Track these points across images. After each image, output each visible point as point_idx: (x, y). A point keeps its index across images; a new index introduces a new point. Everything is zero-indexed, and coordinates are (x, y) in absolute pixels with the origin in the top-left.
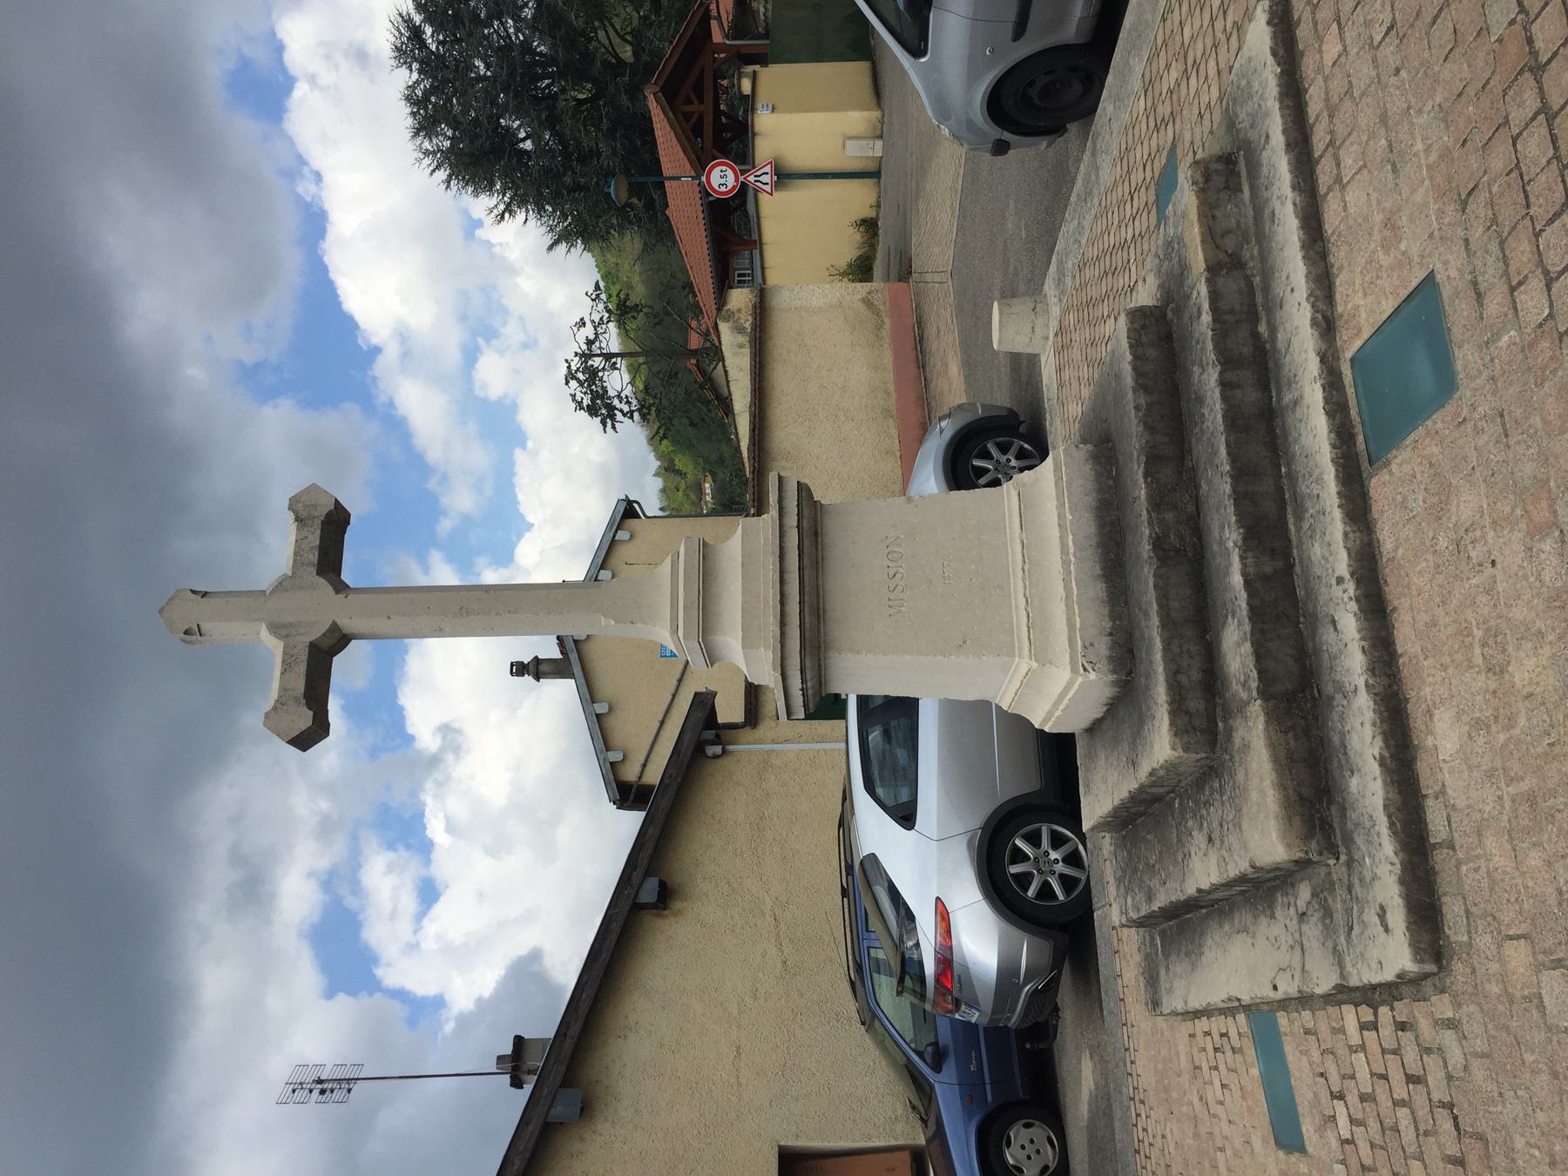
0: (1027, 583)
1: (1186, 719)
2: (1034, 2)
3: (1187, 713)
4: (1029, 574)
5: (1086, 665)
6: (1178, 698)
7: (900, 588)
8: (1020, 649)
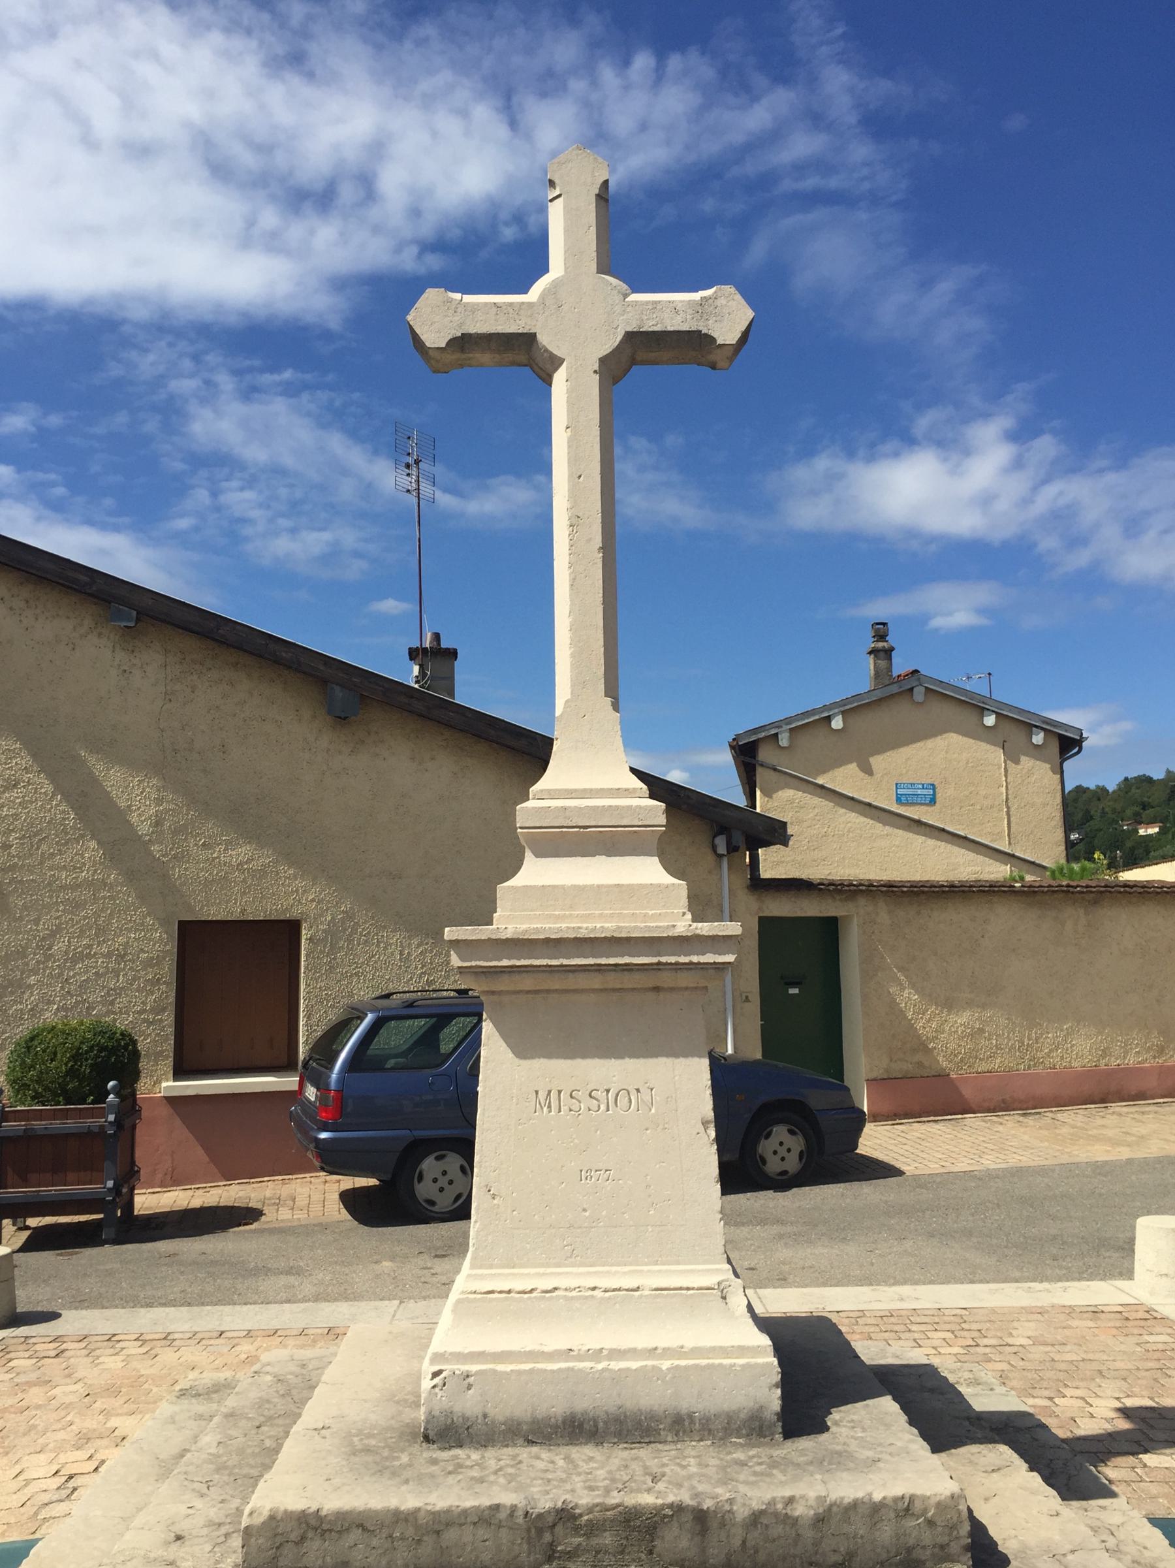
0: (574, 1294)
1: (294, 1536)
2: (1173, 1549)
3: (303, 1538)
4: (586, 1298)
5: (442, 1376)
6: (325, 1527)
7: (575, 1107)
8: (482, 1277)
